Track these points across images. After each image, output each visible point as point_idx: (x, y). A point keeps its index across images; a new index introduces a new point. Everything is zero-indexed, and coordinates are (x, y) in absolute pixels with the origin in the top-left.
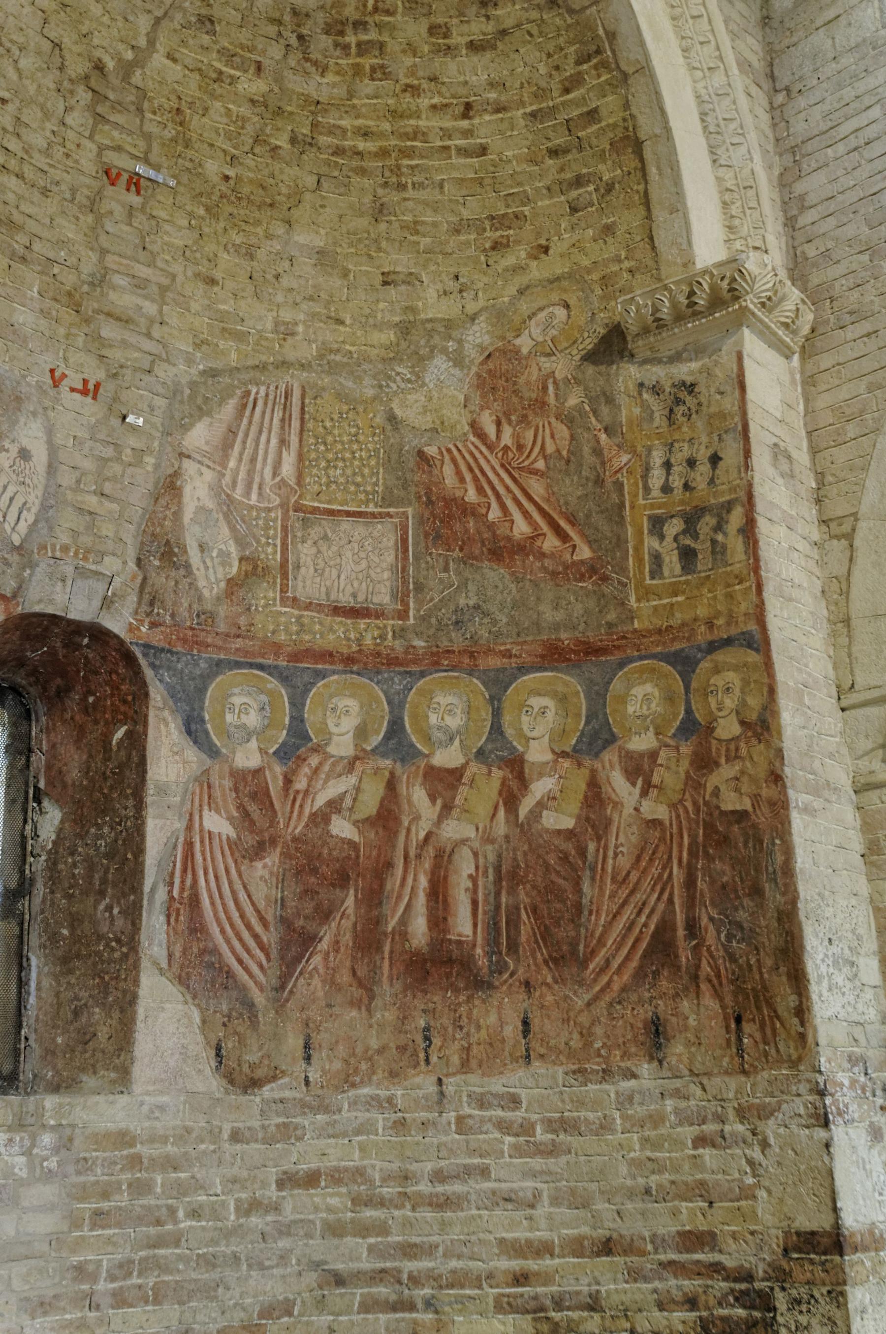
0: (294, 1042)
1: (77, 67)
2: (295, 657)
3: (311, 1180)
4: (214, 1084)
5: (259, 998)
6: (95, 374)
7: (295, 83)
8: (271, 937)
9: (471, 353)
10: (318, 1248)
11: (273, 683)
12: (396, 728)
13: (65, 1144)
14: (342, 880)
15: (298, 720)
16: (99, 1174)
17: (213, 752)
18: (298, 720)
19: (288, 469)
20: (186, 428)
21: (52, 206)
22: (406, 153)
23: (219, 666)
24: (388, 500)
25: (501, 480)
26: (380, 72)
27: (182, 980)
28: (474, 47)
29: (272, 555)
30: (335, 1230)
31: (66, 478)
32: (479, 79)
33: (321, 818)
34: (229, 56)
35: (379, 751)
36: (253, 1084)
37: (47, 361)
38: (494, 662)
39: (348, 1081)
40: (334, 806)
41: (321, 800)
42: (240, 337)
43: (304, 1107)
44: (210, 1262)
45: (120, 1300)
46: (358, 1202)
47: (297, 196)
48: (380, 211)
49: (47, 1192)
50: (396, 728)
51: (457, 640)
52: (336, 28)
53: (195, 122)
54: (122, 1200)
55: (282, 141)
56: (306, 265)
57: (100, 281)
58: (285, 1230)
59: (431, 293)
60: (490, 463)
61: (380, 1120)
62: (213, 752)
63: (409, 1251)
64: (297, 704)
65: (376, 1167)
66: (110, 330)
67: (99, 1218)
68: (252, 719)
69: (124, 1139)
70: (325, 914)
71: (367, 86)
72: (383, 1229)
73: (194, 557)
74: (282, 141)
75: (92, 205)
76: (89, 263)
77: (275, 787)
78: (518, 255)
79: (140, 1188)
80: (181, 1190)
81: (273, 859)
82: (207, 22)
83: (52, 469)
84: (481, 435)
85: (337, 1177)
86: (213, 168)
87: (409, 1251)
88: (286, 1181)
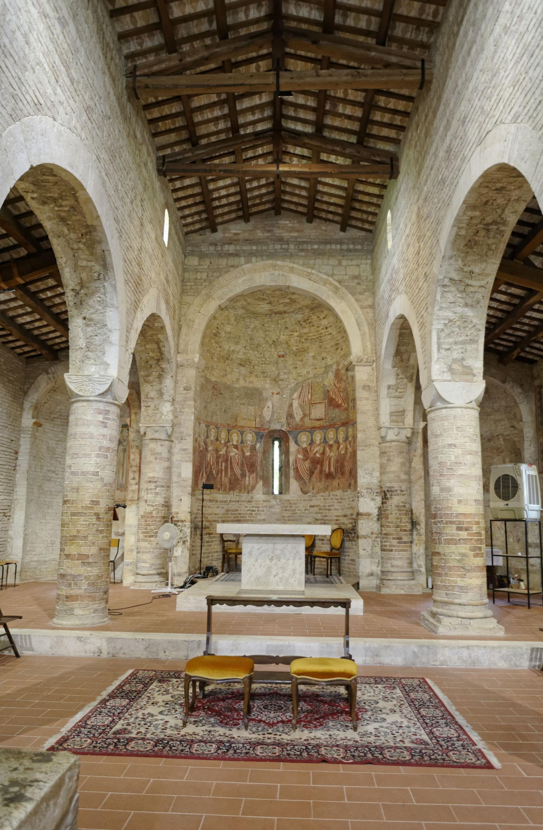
0: (311, 487)
1: (271, 342)
2: (311, 428)
3: (313, 506)
4: (300, 493)
6: (279, 390)
7: (302, 331)
8: (308, 472)
9: (334, 370)
10: (314, 515)
11: (308, 433)
12: (325, 438)
13: (281, 501)
14: (318, 463)
15: (312, 439)
16: (285, 505)
18: (312, 439)
19: (309, 397)
20: (293, 395)
21: (270, 366)
22: (321, 337)
23: (300, 432)
24: (324, 399)
25: (337, 393)
26: (313, 326)
27: (296, 479)
28: (324, 318)
29: (308, 412)
30: (317, 513)
31: (275, 408)
32: (326, 323)
33: (315, 454)
34: (291, 331)
35: (323, 442)
36: (306, 493)
37: (271, 391)
38: (337, 426)
39: (318, 493)
40: (317, 452)
42: (301, 376)
43: (313, 496)
44: (300, 516)
45: (289, 520)
46: (320, 509)
47: (308, 348)
48: (320, 347)
49: (278, 507)
50: (325, 438)
51: (332, 423)
52: (305, 321)
53: (290, 343)
54: (289, 508)
55: (303, 340)
56: (311, 361)
57: (279, 374)
58: (310, 513)
59: (329, 359)
60: (336, 390)
61: (322, 498)
63: (325, 516)
64: (312, 436)
65: (322, 505)
66: (280, 383)
67: (286, 510)
68: (305, 440)
69: (289, 500)
70: (316, 469)
71: (312, 328)
72: (322, 513)
73: (295, 415)
74: (303, 340)
75: (277, 363)
76: (277, 372)
77: (308, 450)
78: (339, 351)
79: (291, 507)
80: (297, 507)
81: (308, 461)
82: (287, 328)
83: (273, 408)
84: (335, 385)
85: (317, 506)
86: (294, 348)
87: (325, 516)
88: (311, 506)
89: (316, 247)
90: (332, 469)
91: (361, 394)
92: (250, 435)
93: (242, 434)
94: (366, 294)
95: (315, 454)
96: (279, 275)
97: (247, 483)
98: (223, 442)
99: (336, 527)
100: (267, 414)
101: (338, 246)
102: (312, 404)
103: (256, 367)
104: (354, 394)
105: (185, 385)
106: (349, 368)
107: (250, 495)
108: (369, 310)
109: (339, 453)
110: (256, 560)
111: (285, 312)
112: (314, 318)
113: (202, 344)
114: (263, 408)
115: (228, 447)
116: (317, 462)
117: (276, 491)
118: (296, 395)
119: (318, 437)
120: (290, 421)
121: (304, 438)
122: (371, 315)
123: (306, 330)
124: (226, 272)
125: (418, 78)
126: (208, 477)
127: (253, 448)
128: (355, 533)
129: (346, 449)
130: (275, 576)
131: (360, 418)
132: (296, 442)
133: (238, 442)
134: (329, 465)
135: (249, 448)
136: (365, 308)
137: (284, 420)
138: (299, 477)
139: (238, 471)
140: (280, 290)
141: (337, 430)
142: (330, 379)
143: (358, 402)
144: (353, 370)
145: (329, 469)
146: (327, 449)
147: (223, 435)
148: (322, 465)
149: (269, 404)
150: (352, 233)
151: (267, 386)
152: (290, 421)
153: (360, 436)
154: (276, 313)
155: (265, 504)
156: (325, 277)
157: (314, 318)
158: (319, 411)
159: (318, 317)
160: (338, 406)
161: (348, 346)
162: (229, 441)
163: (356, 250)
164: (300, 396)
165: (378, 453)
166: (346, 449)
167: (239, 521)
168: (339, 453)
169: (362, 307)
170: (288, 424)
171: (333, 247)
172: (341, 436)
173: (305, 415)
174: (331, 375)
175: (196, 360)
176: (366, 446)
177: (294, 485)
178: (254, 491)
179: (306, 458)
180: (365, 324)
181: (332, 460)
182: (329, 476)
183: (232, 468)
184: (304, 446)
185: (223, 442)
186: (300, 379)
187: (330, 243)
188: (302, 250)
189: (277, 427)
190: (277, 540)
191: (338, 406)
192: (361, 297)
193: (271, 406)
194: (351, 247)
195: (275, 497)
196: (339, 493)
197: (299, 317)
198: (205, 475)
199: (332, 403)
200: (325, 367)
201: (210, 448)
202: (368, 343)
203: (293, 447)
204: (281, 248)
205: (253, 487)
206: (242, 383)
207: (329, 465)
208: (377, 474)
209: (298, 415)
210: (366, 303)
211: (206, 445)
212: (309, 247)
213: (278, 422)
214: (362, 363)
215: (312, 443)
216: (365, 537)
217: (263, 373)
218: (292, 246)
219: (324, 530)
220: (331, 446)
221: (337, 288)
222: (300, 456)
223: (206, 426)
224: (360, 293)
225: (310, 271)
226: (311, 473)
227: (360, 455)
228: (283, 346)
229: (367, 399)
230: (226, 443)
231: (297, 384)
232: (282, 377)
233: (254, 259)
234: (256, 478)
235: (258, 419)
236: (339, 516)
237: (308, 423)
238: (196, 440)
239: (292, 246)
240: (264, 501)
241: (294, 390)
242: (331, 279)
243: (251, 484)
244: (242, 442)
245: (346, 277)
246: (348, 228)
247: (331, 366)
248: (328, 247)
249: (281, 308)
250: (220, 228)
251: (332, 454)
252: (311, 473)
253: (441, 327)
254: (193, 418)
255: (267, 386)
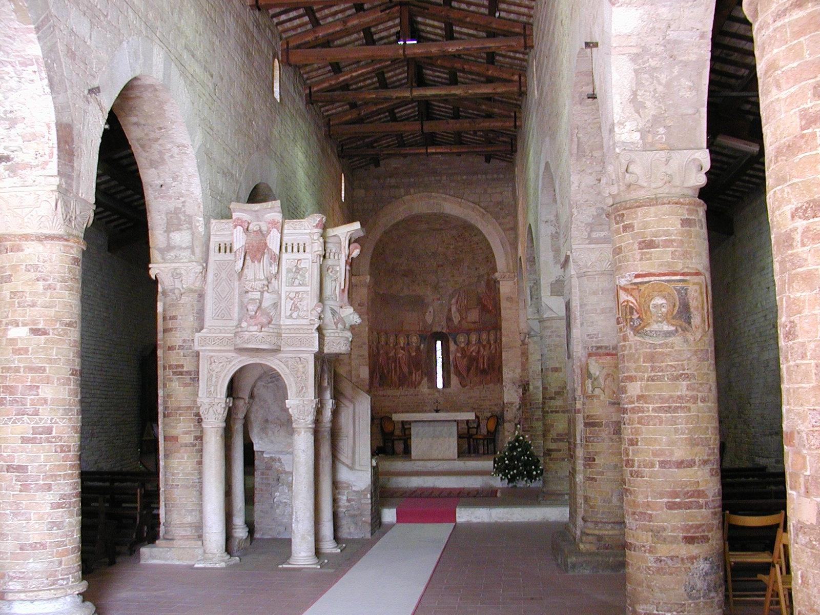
4: (459, 386)
5: (465, 376)
6: (439, 296)
17: (458, 346)
19: (466, 303)
24: (478, 305)
33: (472, 352)
34: (448, 244)
41: (471, 350)
48: (474, 258)
57: (438, 282)
62: (458, 346)
66: (440, 290)
68: (463, 340)
71: (466, 243)
73: (454, 319)
75: (436, 272)
86: (451, 259)
87: (481, 406)
89: (465, 177)
90: (485, 366)
91: (504, 304)
92: (415, 338)
93: (408, 338)
94: (508, 218)
95: (472, 352)
96: (434, 203)
97: (414, 378)
98: (391, 345)
99: (489, 415)
100: (429, 319)
101: (484, 176)
102: (468, 309)
103: (418, 276)
104: (500, 304)
105: (359, 302)
106: (496, 282)
107: (417, 389)
108: (510, 232)
109: (491, 352)
110: (422, 439)
111: (442, 229)
112: (467, 234)
113: (371, 264)
114: (426, 313)
115: (396, 349)
116: (473, 360)
117: (440, 385)
118: (454, 301)
119: (474, 338)
120: (450, 324)
121: (462, 339)
122: (513, 236)
123: (460, 244)
124: (390, 203)
125: (513, 124)
126: (381, 376)
127: (418, 349)
128: (503, 418)
129: (496, 350)
130: (436, 450)
131: (504, 325)
132: (455, 343)
133: (404, 344)
134: (483, 363)
135: (414, 349)
136: (508, 230)
137: (444, 323)
138: (458, 374)
139: (406, 370)
140: (435, 214)
141: (489, 333)
142: (482, 288)
143: (503, 312)
144: (499, 284)
145: (484, 366)
146: (482, 349)
147: (392, 339)
148: (477, 363)
149: (431, 309)
150: (495, 163)
151: (429, 293)
152: (450, 324)
153: (503, 339)
154: (434, 230)
155: (430, 397)
156: (473, 205)
157: (467, 234)
158: (474, 315)
159: (470, 234)
160: (489, 312)
161: (495, 262)
162: (397, 344)
163: (499, 180)
164: (457, 302)
165: (520, 353)
166: (496, 350)
167: (407, 412)
168: (491, 352)
169: (504, 230)
170: (448, 327)
171: (480, 177)
172: (492, 337)
173: (462, 318)
174: (483, 283)
175: (368, 281)
176: (510, 348)
177: (454, 380)
178: (420, 387)
179: (464, 357)
180: (508, 244)
181: (486, 358)
182: (483, 372)
183: (400, 367)
184: (462, 345)
185: (391, 345)
186: (457, 286)
187: (476, 174)
188: (452, 181)
189: (439, 330)
190: (436, 424)
191: (489, 312)
192: (504, 220)
193: (432, 311)
194: (495, 176)
195: (439, 390)
196: (491, 385)
197: (454, 232)
198: (378, 375)
199: (484, 309)
200: (479, 277)
201: (381, 352)
202: (511, 261)
203: (453, 347)
204: (435, 180)
205: (420, 383)
206: (406, 292)
207: (483, 363)
208: (518, 371)
209: (456, 318)
210: (508, 226)
211: (378, 350)
212: (459, 178)
213: (439, 325)
214: (505, 279)
215: (468, 343)
216: (510, 421)
217: (424, 281)
218: (444, 178)
219: (471, 416)
220: (484, 346)
221: (483, 214)
222: (459, 355)
223: (378, 334)
224: (503, 218)
225: (460, 200)
226: (469, 370)
227: (504, 355)
228: (441, 256)
229: (510, 309)
230: (394, 346)
231: (455, 291)
232: (441, 284)
233: (412, 191)
234: (422, 375)
235: (421, 324)
236: (491, 405)
237: (465, 325)
238: (370, 347)
239: (444, 178)
240: (429, 394)
241: (452, 296)
242: (477, 206)
243: (417, 380)
244: (408, 344)
245: (492, 204)
246: (492, 160)
247: (483, 276)
248: (475, 178)
249: (438, 226)
250: (382, 163)
251: (485, 353)
252: (469, 370)
253: (532, 285)
254: (367, 329)
255: (428, 294)
